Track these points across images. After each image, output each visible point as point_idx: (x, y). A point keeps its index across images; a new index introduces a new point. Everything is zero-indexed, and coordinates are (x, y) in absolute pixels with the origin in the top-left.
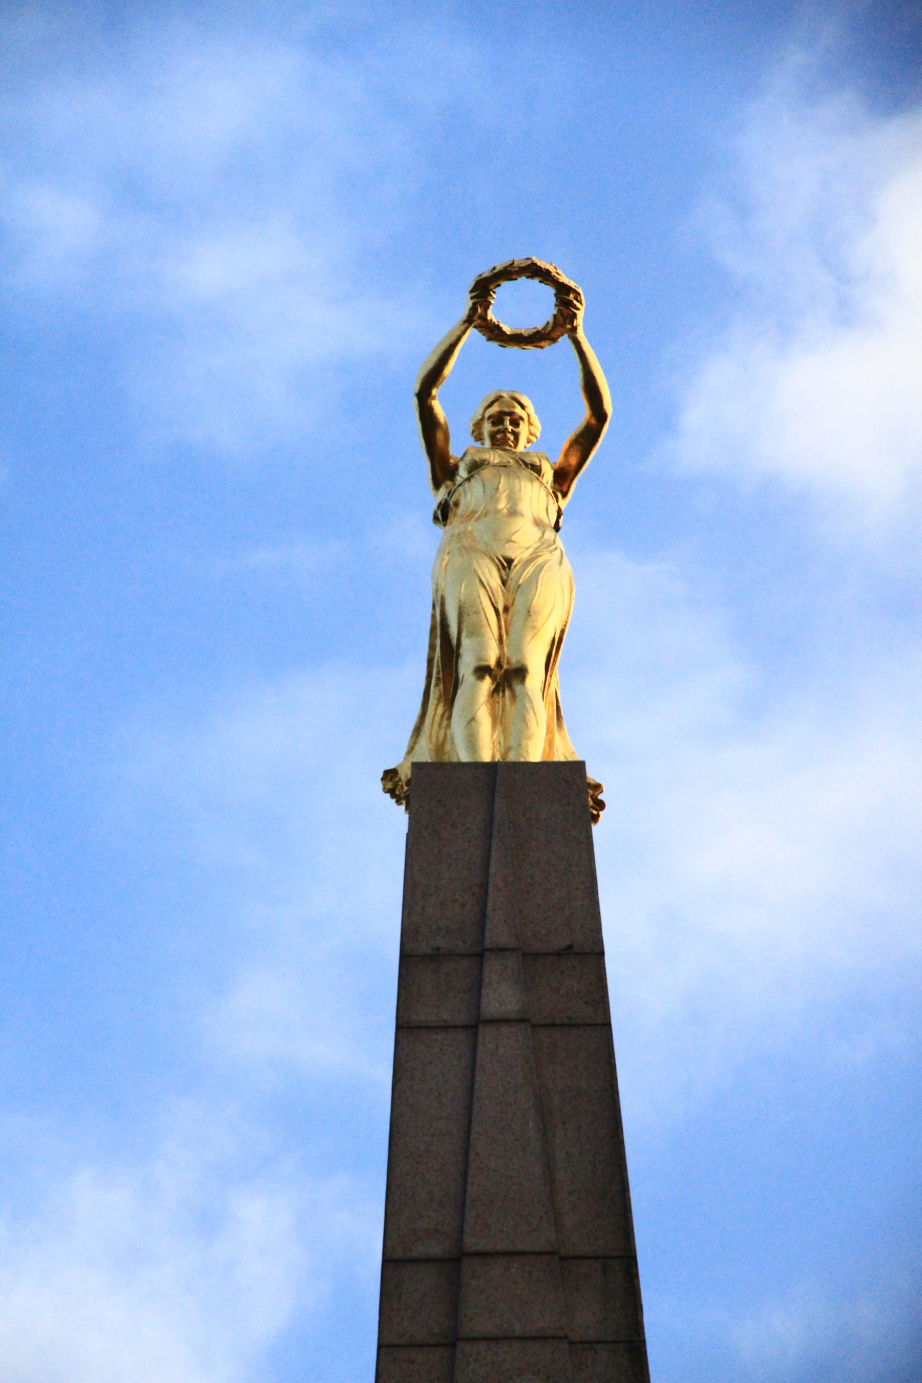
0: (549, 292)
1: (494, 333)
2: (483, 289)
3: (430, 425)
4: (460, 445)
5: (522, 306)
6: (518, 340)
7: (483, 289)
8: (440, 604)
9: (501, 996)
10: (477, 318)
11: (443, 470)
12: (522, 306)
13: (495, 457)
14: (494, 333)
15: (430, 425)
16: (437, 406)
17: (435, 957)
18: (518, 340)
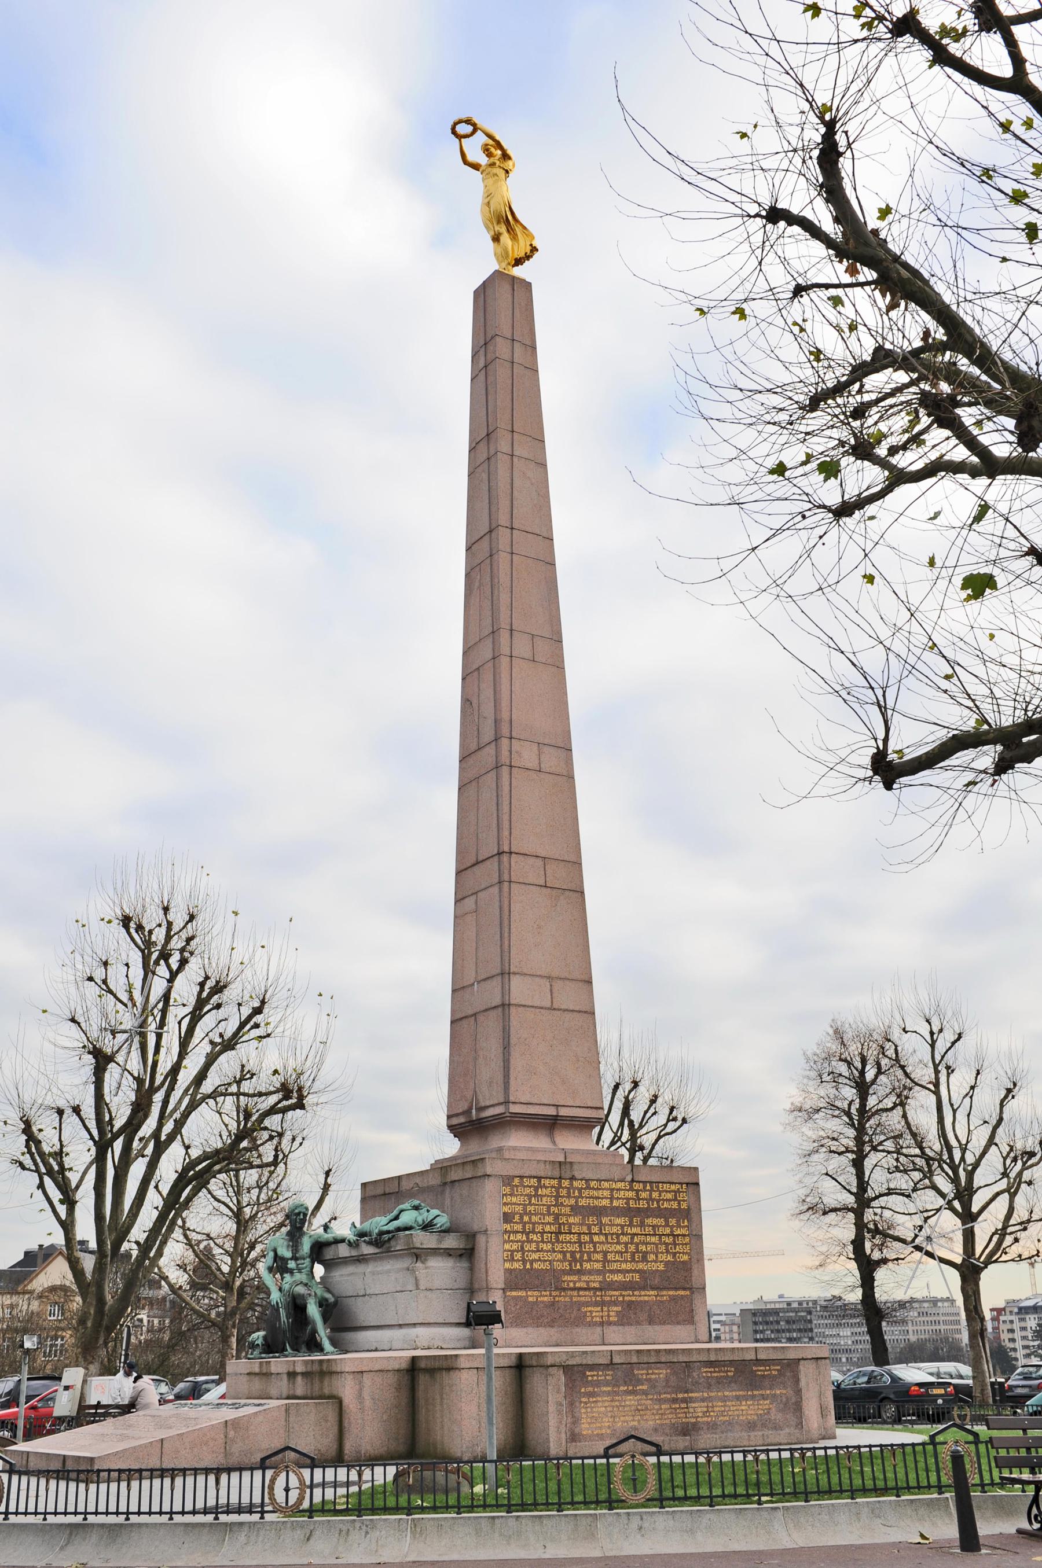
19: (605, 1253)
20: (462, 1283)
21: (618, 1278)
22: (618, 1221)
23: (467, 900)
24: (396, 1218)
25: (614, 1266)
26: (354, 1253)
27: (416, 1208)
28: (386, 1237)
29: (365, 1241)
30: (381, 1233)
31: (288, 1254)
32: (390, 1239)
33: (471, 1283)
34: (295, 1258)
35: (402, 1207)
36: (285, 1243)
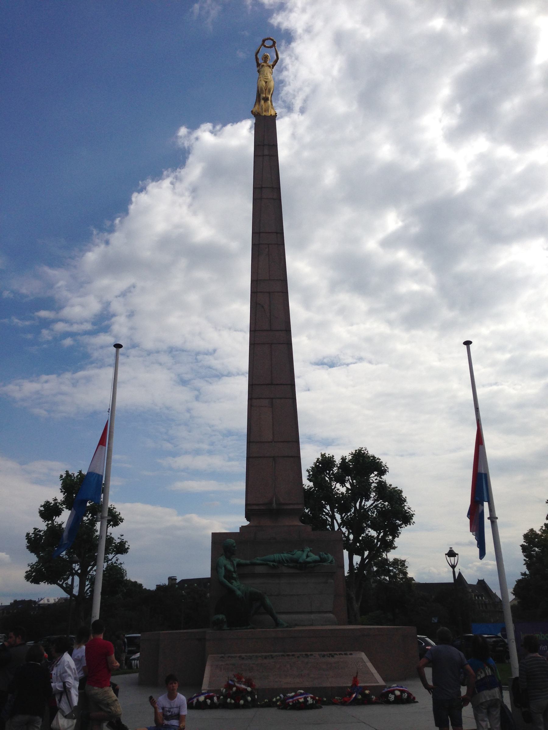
0: (272, 42)
1: (265, 46)
2: (264, 41)
3: (257, 59)
4: (260, 61)
5: (268, 43)
6: (268, 47)
8: (258, 87)
9: (266, 152)
10: (263, 44)
11: (258, 65)
12: (268, 43)
13: (265, 64)
14: (265, 46)
15: (257, 59)
16: (258, 56)
17: (259, 145)
18: (268, 47)
31: (232, 570)
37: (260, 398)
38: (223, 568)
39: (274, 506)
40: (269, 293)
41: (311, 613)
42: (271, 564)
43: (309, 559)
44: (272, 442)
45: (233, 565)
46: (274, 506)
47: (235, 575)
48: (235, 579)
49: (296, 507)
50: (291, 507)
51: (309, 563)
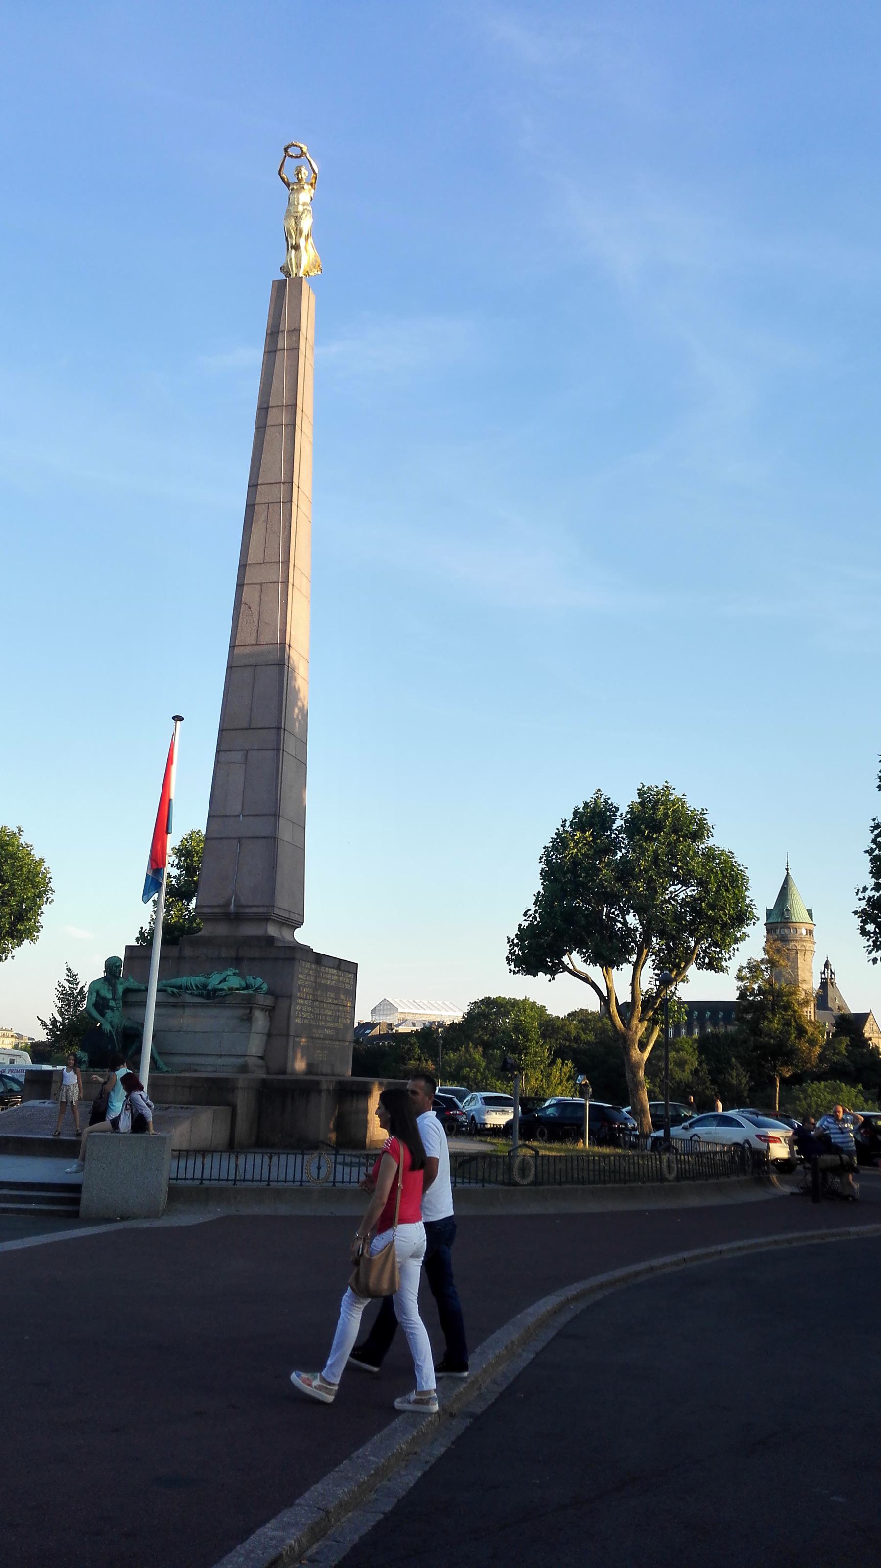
2: (286, 150)
7: (286, 150)
15: (283, 179)
19: (326, 1015)
20: (266, 1031)
21: (328, 1032)
22: (332, 995)
23: (233, 753)
24: (224, 980)
25: (329, 1024)
26: (172, 1000)
27: (235, 974)
28: (223, 993)
29: (192, 994)
30: (215, 990)
31: (109, 996)
32: (226, 995)
33: (270, 1030)
34: (114, 999)
35: (228, 973)
36: (106, 987)
37: (231, 751)
38: (95, 994)
39: (232, 908)
40: (261, 584)
41: (221, 1056)
42: (170, 990)
43: (224, 986)
44: (239, 816)
45: (114, 991)
46: (232, 908)
47: (112, 1003)
48: (112, 1009)
49: (261, 910)
50: (254, 910)
51: (222, 990)
